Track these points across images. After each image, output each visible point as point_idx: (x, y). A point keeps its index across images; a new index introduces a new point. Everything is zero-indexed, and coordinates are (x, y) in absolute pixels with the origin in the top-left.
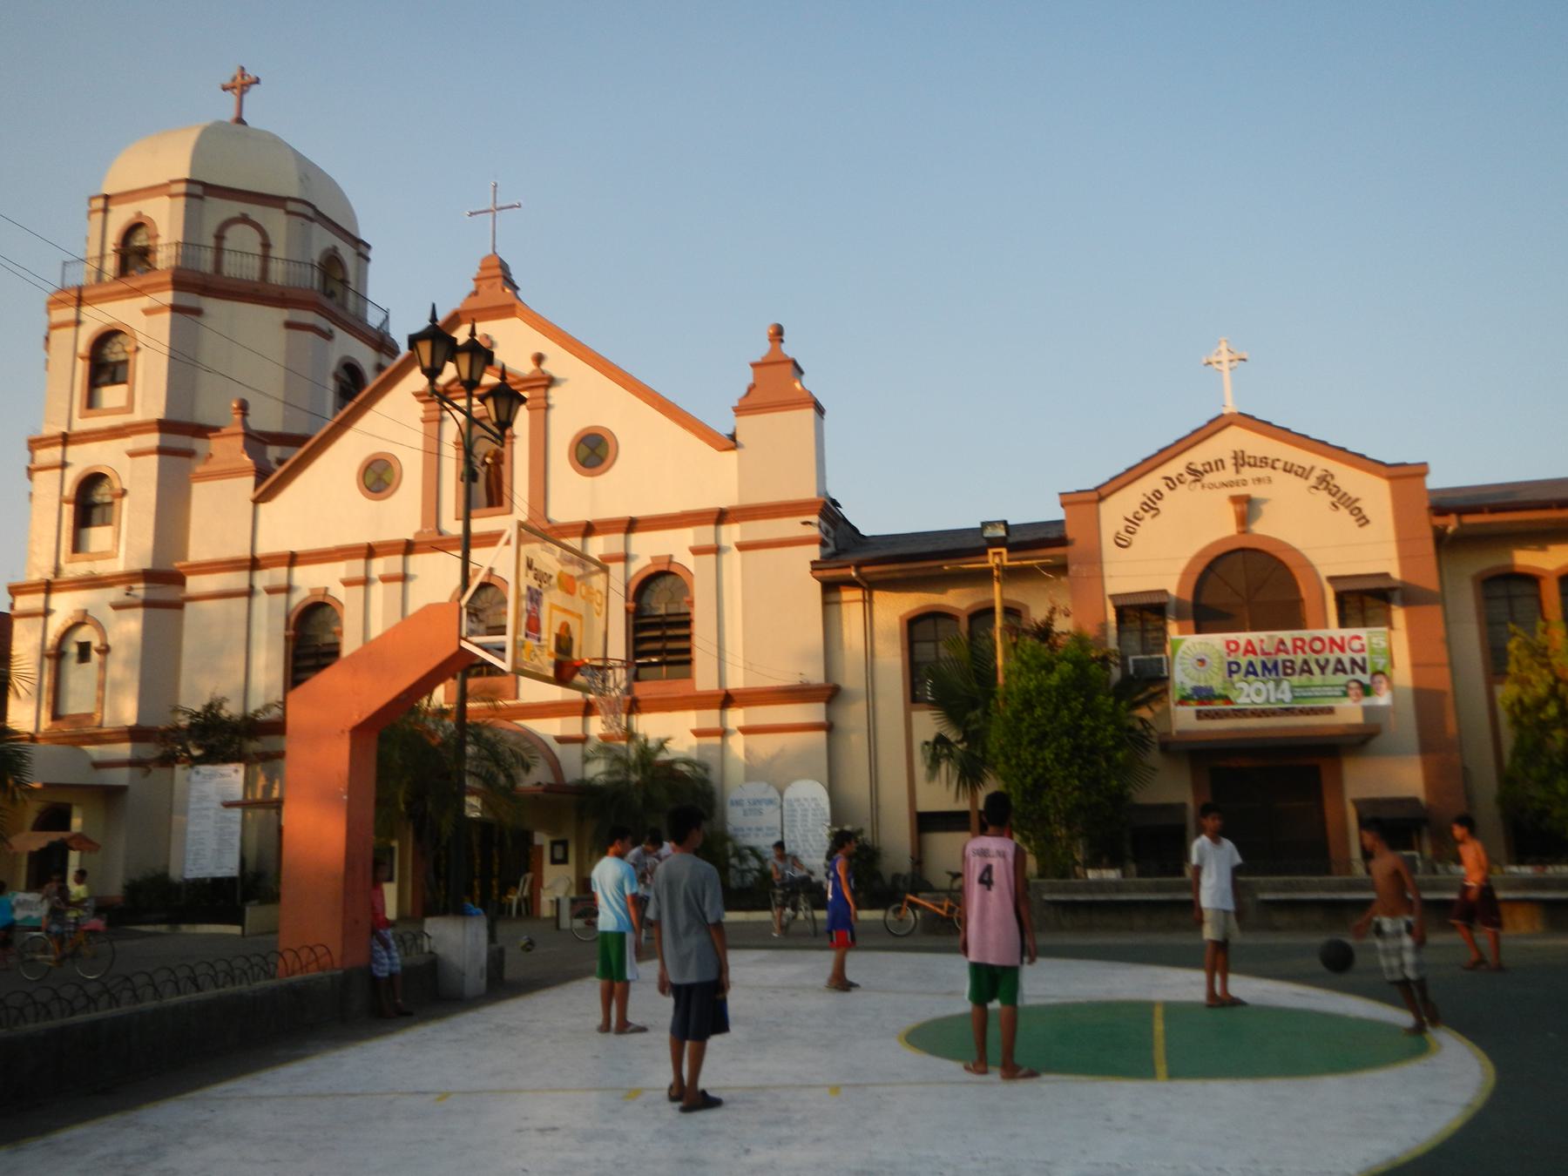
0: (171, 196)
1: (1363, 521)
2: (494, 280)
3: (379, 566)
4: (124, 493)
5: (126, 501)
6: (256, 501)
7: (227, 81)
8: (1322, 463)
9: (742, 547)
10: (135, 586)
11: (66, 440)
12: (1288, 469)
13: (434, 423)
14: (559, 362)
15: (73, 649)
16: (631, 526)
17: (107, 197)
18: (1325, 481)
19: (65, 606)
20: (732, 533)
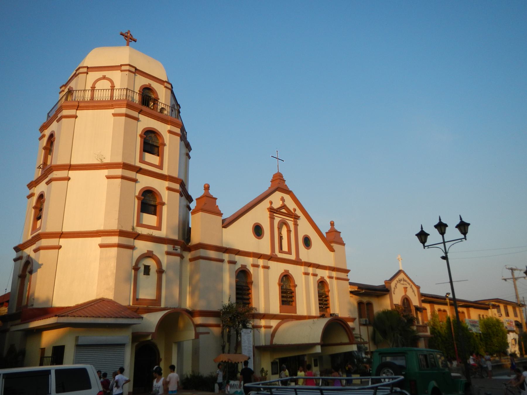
0: (166, 87)
1: (415, 296)
2: (283, 181)
3: (261, 262)
4: (163, 204)
5: (165, 208)
6: (223, 227)
7: (124, 32)
8: (411, 284)
9: (338, 279)
10: (176, 246)
11: (139, 170)
12: (408, 283)
13: (272, 218)
14: (299, 213)
15: (142, 268)
16: (318, 266)
17: (136, 69)
18: (411, 286)
19: (142, 246)
20: (334, 274)
